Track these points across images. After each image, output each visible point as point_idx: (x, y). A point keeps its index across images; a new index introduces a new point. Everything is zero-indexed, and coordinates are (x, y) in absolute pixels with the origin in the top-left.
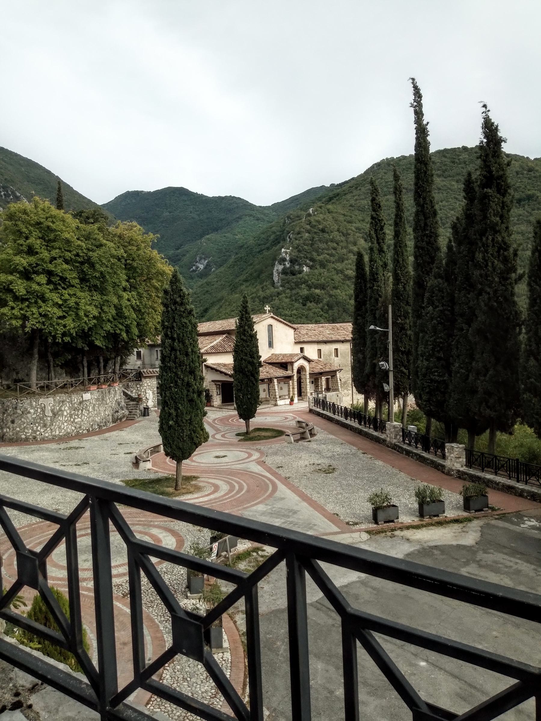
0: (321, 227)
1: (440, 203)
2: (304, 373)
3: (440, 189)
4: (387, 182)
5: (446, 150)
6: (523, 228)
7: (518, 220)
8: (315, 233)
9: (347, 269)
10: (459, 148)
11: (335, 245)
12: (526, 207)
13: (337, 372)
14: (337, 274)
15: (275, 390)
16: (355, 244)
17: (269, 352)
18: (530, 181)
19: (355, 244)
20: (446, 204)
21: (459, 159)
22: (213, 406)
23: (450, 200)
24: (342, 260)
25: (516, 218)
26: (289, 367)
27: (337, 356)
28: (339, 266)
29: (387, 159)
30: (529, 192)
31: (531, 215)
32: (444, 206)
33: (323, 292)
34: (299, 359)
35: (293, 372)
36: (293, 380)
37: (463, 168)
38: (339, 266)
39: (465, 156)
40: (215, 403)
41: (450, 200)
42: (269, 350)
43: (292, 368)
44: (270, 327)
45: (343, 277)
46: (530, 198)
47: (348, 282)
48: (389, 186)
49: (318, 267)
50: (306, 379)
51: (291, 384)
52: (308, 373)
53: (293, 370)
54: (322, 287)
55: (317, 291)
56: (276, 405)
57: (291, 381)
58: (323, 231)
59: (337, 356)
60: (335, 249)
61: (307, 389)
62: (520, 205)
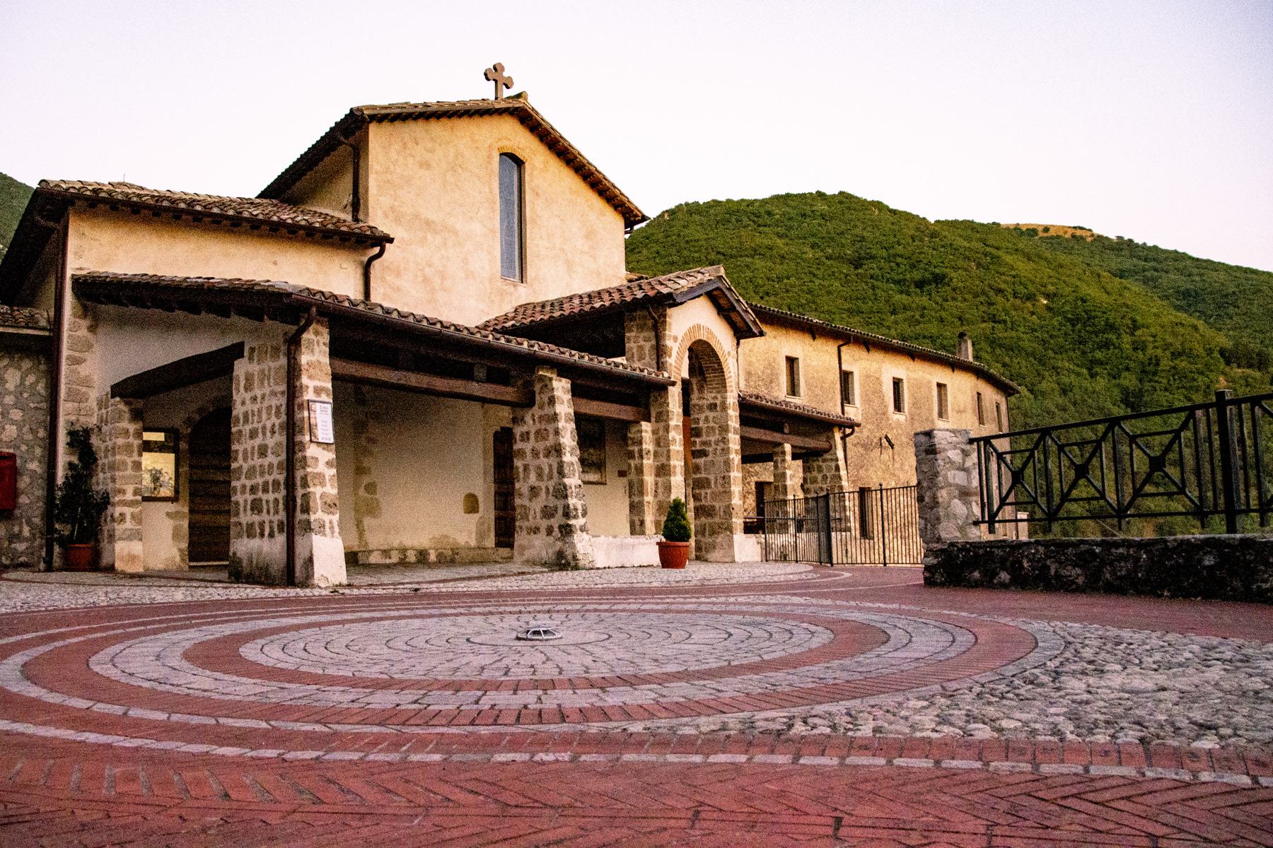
1: (785, 281)
2: (709, 397)
3: (783, 257)
4: (687, 242)
5: (788, 195)
7: (922, 316)
10: (811, 194)
13: (838, 436)
15: (558, 450)
17: (502, 294)
18: (934, 252)
22: (111, 569)
26: (637, 340)
27: (793, 389)
29: (687, 204)
30: (937, 271)
32: (793, 286)
34: (699, 296)
35: (660, 366)
36: (663, 417)
37: (820, 225)
39: (821, 207)
40: (121, 548)
41: (803, 276)
42: (500, 283)
43: (659, 338)
44: (514, 161)
46: (939, 279)
48: (692, 249)
50: (724, 429)
51: (648, 445)
52: (732, 399)
53: (660, 351)
56: (563, 562)
57: (646, 426)
59: (793, 389)
61: (728, 493)
62: (922, 292)
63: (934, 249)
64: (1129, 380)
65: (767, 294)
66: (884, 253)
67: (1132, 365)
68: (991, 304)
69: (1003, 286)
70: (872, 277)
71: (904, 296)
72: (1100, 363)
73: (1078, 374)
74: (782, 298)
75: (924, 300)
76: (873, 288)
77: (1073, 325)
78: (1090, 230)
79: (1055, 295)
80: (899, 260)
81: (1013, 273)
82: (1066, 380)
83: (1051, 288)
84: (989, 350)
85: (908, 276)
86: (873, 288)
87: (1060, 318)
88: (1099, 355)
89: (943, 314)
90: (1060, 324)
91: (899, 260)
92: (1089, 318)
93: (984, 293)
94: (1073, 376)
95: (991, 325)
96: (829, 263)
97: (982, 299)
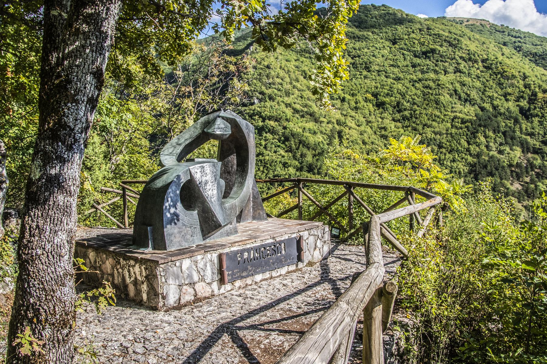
0: (266, 64)
3: (359, 38)
6: (432, 76)
8: (261, 69)
9: (295, 103)
11: (281, 81)
12: (432, 58)
14: (287, 107)
16: (297, 80)
19: (297, 80)
20: (368, 51)
21: (371, 15)
23: (370, 47)
24: (288, 94)
25: (425, 68)
28: (287, 100)
31: (436, 65)
33: (276, 123)
38: (287, 100)
41: (370, 47)
45: (292, 111)
46: (433, 51)
47: (297, 115)
49: (267, 99)
54: (277, 120)
55: (272, 123)
58: (268, 67)
60: (281, 84)
63: (430, 36)
64: (524, 103)
65: (355, 57)
66: (407, 37)
67: (525, 95)
68: (458, 64)
69: (464, 55)
70: (402, 49)
71: (418, 59)
72: (510, 94)
73: (500, 100)
74: (362, 59)
75: (428, 62)
76: (403, 54)
77: (496, 75)
78: (488, 21)
79: (487, 59)
80: (415, 41)
81: (468, 48)
82: (495, 103)
83: (485, 57)
84: (460, 87)
85: (419, 49)
86: (403, 54)
87: (490, 71)
88: (509, 90)
89: (437, 68)
90: (491, 75)
91: (415, 41)
92: (504, 72)
93: (454, 58)
94: (498, 100)
95: (458, 74)
96: (381, 41)
97: (454, 61)
